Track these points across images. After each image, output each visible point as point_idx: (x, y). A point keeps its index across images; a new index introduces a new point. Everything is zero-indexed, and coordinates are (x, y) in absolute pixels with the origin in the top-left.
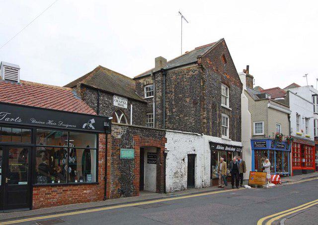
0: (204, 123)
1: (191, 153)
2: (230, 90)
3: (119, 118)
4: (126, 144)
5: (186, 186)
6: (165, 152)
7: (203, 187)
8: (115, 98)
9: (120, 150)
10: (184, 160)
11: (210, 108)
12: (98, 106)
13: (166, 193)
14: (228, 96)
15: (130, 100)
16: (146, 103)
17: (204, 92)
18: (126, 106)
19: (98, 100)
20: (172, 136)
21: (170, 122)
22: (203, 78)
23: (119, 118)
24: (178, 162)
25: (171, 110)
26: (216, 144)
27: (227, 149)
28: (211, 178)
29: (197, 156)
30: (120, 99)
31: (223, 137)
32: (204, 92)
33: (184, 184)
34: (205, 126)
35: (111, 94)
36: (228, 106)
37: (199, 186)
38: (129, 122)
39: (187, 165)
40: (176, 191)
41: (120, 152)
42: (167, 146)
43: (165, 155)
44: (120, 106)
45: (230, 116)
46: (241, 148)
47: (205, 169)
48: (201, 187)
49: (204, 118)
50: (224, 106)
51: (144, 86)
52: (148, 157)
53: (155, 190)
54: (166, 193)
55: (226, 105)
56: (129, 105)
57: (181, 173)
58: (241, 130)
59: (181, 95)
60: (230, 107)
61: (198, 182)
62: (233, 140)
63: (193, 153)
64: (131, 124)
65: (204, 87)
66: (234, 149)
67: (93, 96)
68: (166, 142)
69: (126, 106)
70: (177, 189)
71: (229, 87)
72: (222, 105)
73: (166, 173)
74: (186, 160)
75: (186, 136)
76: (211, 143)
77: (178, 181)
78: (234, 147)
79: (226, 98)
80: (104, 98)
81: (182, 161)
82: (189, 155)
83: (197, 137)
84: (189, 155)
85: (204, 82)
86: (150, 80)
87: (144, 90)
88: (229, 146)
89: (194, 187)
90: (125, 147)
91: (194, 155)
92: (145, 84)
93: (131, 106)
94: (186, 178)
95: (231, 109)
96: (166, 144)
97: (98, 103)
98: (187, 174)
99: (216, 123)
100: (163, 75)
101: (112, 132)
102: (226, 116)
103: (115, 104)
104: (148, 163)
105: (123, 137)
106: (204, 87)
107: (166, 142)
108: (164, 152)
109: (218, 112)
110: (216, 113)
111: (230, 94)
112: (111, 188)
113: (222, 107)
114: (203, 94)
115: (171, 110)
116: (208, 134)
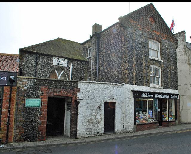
0: (125, 73)
1: (108, 101)
2: (160, 45)
3: (59, 75)
4: (32, 94)
5: (102, 131)
6: (78, 101)
7: (124, 133)
8: (55, 59)
9: (25, 100)
10: (99, 107)
11: (133, 60)
12: (36, 66)
13: (76, 138)
14: (159, 50)
15: (70, 60)
16: (88, 62)
17: (126, 46)
18: (66, 65)
19: (36, 61)
20: (86, 86)
21: (102, 76)
22: (124, 36)
23: (59, 75)
24: (92, 110)
25: (103, 66)
26: (141, 93)
27: (156, 96)
28: (135, 123)
29: (117, 104)
30: (60, 60)
31: (152, 85)
32: (126, 46)
33: (100, 130)
34: (126, 76)
35: (52, 56)
36: (159, 59)
37: (118, 132)
38: (69, 78)
39: (103, 112)
40: (91, 136)
41: (25, 101)
42: (79, 95)
43: (77, 103)
44: (60, 65)
45: (161, 67)
46: (177, 95)
47: (126, 115)
48: (122, 133)
49: (125, 70)
50: (155, 58)
51: (87, 49)
52: (68, 106)
53: (69, 136)
54: (76, 138)
55: (158, 58)
56: (69, 64)
57: (96, 120)
58: (177, 79)
59: (109, 52)
60: (161, 59)
61: (118, 127)
62: (166, 87)
63: (112, 101)
64: (70, 79)
65: (126, 42)
66: (168, 97)
67: (32, 58)
68: (79, 92)
69: (66, 65)
70: (92, 135)
71: (160, 42)
72: (150, 57)
73: (78, 120)
74: (103, 108)
75: (103, 86)
76: (134, 92)
77: (93, 127)
78: (167, 94)
79: (158, 52)
80: (42, 60)
81: (98, 109)
82: (106, 104)
83: (116, 87)
84: (106, 104)
85: (125, 38)
86: (90, 43)
87: (87, 51)
88: (159, 94)
89: (114, 132)
90: (31, 98)
91: (114, 104)
92: (88, 47)
93: (71, 64)
94: (102, 124)
95: (162, 61)
96: (78, 94)
97: (37, 64)
98: (103, 121)
99: (142, 74)
100: (97, 37)
101: (18, 85)
102: (157, 67)
103: (54, 63)
104: (67, 111)
105: (28, 88)
106: (126, 42)
107: (79, 92)
108: (76, 101)
110: (143, 65)
111: (161, 48)
112: (12, 135)
114: (125, 48)
115: (103, 66)
116: (130, 83)
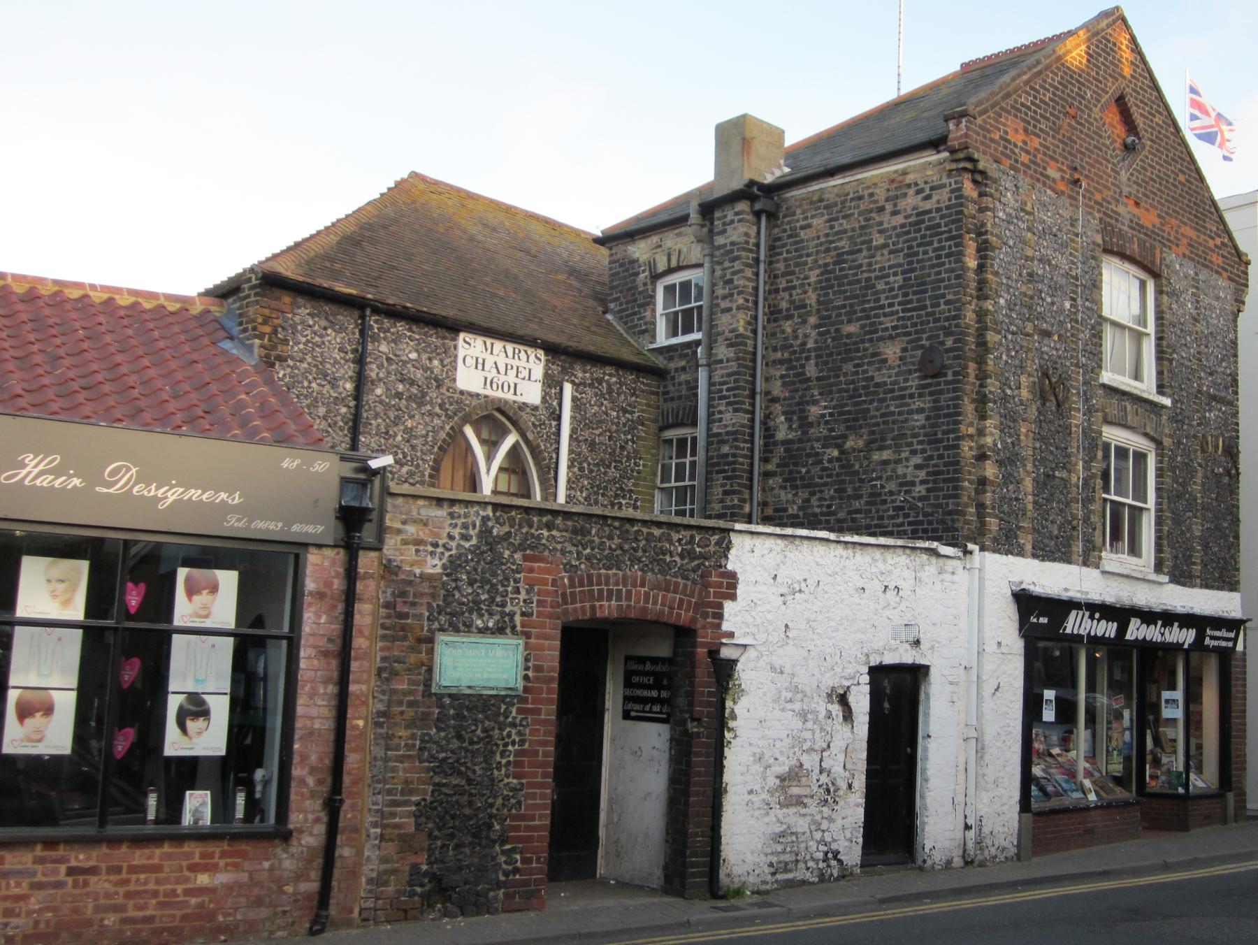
1: (889, 659)
2: (1159, 292)
3: (489, 458)
4: (475, 607)
5: (852, 854)
6: (725, 653)
8: (470, 347)
9: (431, 640)
11: (1025, 394)
12: (358, 394)
14: (1151, 328)
18: (532, 394)
21: (791, 482)
24: (804, 716)
26: (1059, 608)
27: (1136, 631)
29: (934, 674)
30: (499, 353)
31: (1113, 560)
33: (841, 845)
36: (1147, 387)
37: (938, 858)
38: (549, 483)
41: (431, 652)
42: (734, 616)
44: (499, 394)
45: (1158, 443)
46: (1235, 625)
47: (980, 751)
48: (958, 862)
50: (1123, 381)
51: (656, 277)
52: (628, 684)
54: (715, 896)
55: (1137, 376)
56: (552, 383)
57: (824, 779)
58: (1236, 521)
59: (852, 328)
60: (1161, 389)
62: (1181, 577)
63: (907, 657)
64: (561, 499)
66: (1186, 637)
67: (333, 338)
68: (733, 597)
69: (532, 394)
70: (800, 874)
71: (1156, 275)
72: (1107, 377)
73: (727, 777)
74: (861, 702)
76: (1026, 602)
78: (1188, 620)
79: (1139, 336)
86: (684, 243)
88: (1149, 617)
89: (914, 861)
90: (468, 627)
92: (661, 266)
93: (568, 389)
94: (852, 810)
95: (1167, 402)
96: (728, 606)
97: (361, 381)
98: (860, 782)
99: (1065, 481)
102: (1134, 441)
103: (468, 380)
104: (627, 716)
105: (453, 566)
107: (733, 597)
108: (713, 653)
109: (1077, 419)
110: (1068, 427)
111: (1159, 317)
113: (1111, 390)
115: (797, 413)
116: (1007, 544)
